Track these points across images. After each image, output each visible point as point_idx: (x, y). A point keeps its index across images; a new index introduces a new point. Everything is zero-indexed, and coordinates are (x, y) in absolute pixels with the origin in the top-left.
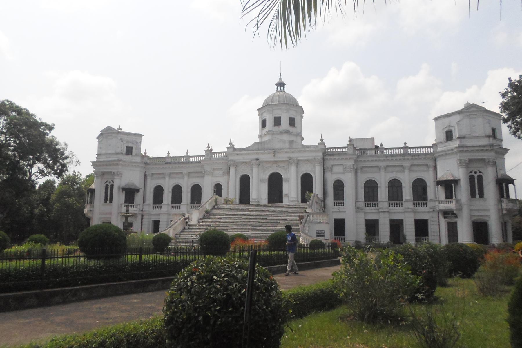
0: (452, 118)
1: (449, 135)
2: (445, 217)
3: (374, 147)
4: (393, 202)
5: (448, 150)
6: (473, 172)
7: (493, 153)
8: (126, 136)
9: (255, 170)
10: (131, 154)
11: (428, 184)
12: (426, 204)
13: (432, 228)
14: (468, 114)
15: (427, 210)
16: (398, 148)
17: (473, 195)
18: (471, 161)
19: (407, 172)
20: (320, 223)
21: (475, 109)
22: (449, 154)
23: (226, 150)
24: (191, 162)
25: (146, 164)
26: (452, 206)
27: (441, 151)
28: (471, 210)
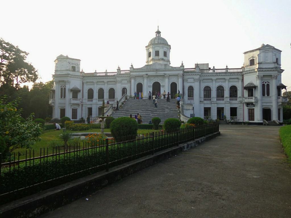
0: (254, 53)
1: (252, 62)
2: (247, 106)
3: (208, 69)
4: (219, 98)
5: (252, 70)
6: (264, 82)
7: (277, 72)
8: (72, 61)
9: (145, 80)
10: (75, 71)
11: (238, 89)
12: (237, 99)
13: (239, 112)
14: (264, 50)
15: (238, 103)
16: (223, 69)
17: (263, 95)
18: (264, 76)
19: (227, 82)
20: (189, 110)
21: (268, 48)
22: (252, 72)
23: (129, 69)
24: (109, 76)
25: (84, 77)
26: (252, 100)
27: (247, 71)
28: (262, 103)
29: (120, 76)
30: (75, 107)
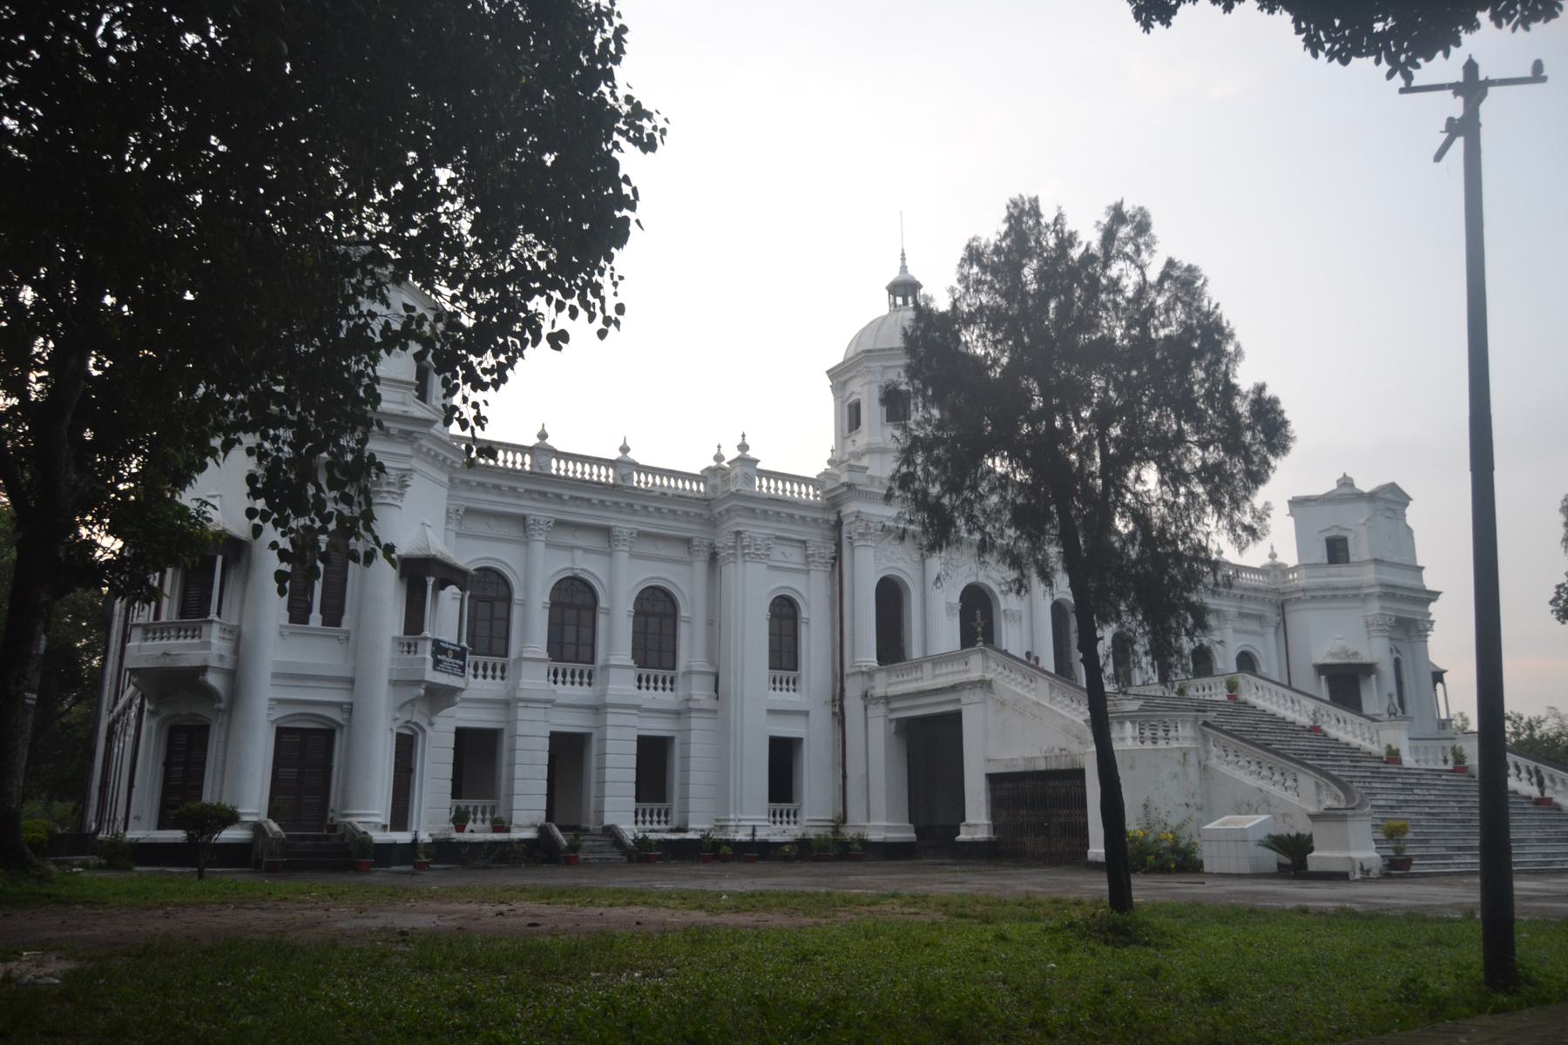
1: (1337, 550)
5: (1347, 588)
22: (1345, 596)
24: (646, 494)
29: (772, 508)
30: (417, 718)
